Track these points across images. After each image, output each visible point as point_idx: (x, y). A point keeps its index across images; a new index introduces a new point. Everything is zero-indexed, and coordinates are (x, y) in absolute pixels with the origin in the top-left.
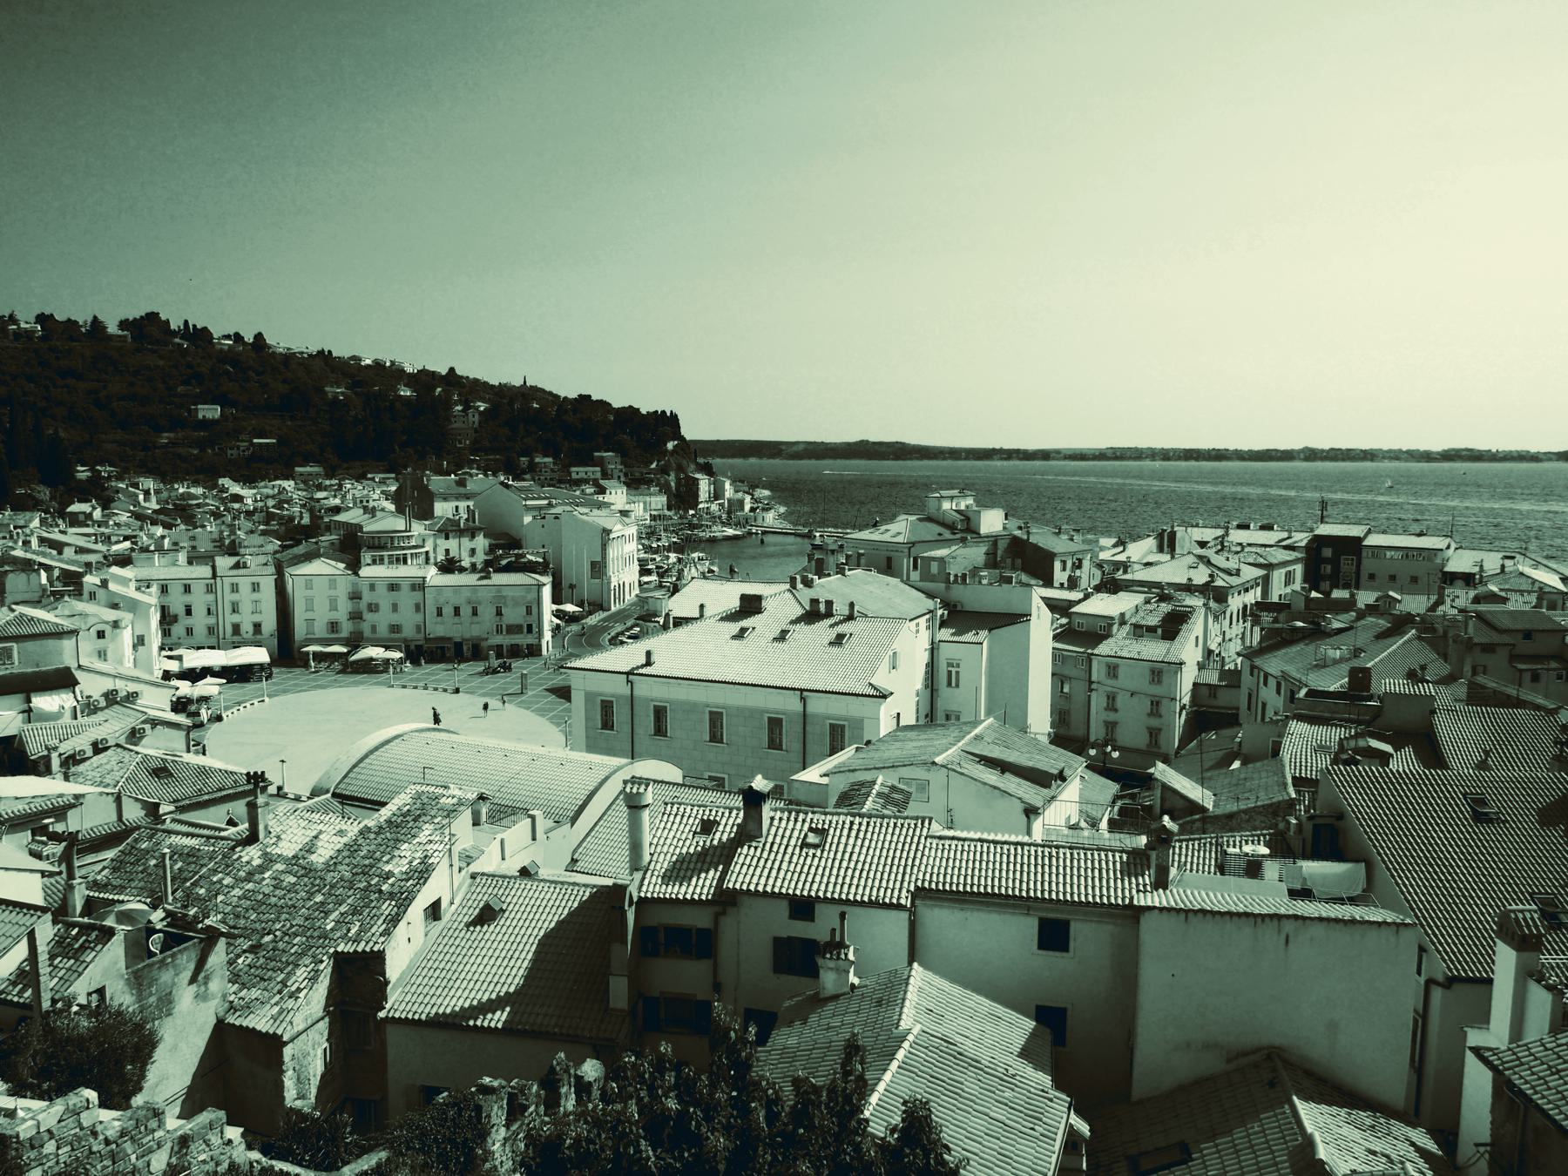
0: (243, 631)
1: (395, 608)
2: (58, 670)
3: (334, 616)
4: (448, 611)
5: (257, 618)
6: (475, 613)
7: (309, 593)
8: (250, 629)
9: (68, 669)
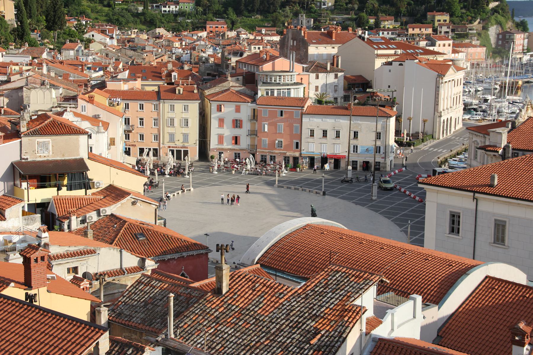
0: (176, 139)
2: (75, 160)
4: (318, 134)
5: (185, 130)
6: (338, 135)
8: (181, 140)
9: (82, 160)
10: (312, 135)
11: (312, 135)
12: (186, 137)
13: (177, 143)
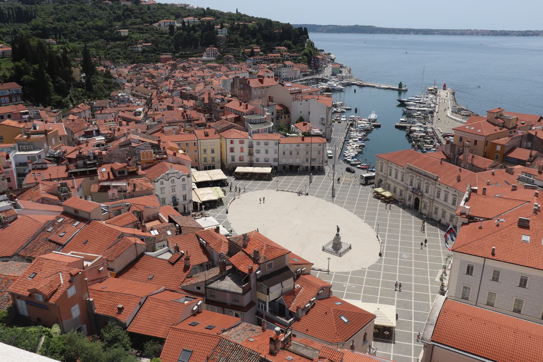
1: (267, 152)
3: (242, 154)
4: (287, 153)
5: (213, 155)
6: (298, 153)
7: (232, 145)
8: (211, 160)
10: (284, 153)
11: (284, 153)
12: (213, 159)
13: (208, 162)
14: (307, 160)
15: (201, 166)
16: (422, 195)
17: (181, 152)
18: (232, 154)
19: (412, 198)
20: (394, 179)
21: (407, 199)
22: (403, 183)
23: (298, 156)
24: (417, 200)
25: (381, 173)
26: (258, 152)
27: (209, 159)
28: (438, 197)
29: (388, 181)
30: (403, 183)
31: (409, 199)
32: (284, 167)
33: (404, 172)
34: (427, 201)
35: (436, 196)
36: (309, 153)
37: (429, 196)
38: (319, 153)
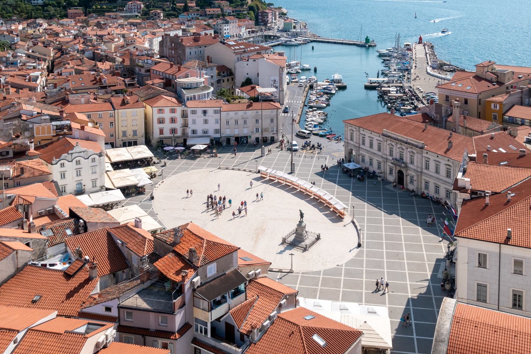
0: (128, 134)
1: (206, 122)
3: (173, 126)
4: (232, 122)
5: (135, 128)
6: (245, 122)
8: (132, 134)
10: (228, 123)
11: (228, 123)
12: (135, 133)
14: (257, 130)
15: (119, 142)
16: (406, 167)
17: (90, 125)
18: (161, 126)
19: (394, 171)
20: (369, 149)
21: (388, 171)
22: (380, 154)
23: (245, 126)
24: (400, 173)
25: (351, 142)
26: (194, 122)
27: (130, 133)
28: (427, 168)
29: (361, 152)
30: (380, 154)
31: (391, 173)
32: (228, 140)
33: (381, 139)
34: (414, 174)
35: (424, 167)
36: (260, 121)
37: (415, 168)
38: (272, 121)
